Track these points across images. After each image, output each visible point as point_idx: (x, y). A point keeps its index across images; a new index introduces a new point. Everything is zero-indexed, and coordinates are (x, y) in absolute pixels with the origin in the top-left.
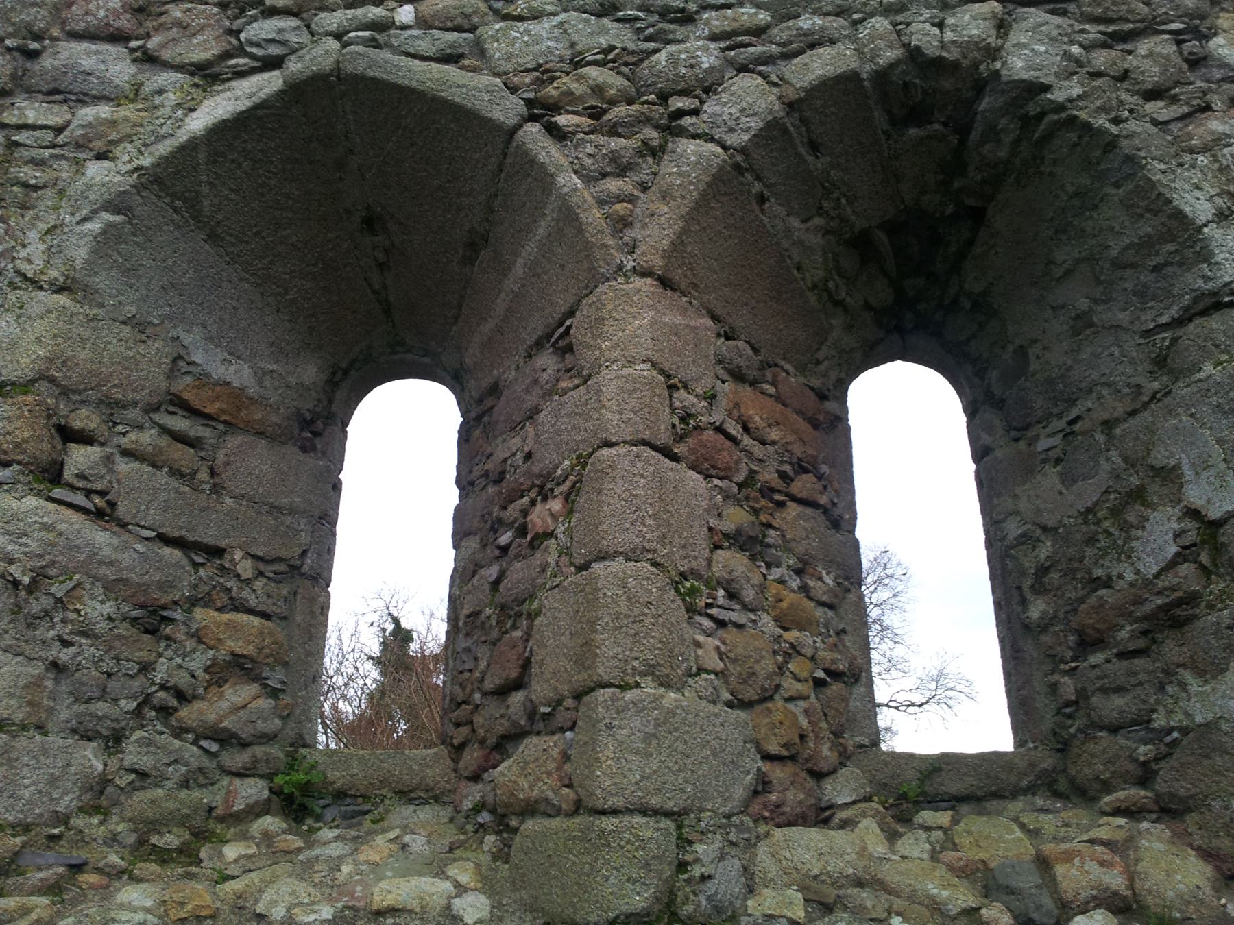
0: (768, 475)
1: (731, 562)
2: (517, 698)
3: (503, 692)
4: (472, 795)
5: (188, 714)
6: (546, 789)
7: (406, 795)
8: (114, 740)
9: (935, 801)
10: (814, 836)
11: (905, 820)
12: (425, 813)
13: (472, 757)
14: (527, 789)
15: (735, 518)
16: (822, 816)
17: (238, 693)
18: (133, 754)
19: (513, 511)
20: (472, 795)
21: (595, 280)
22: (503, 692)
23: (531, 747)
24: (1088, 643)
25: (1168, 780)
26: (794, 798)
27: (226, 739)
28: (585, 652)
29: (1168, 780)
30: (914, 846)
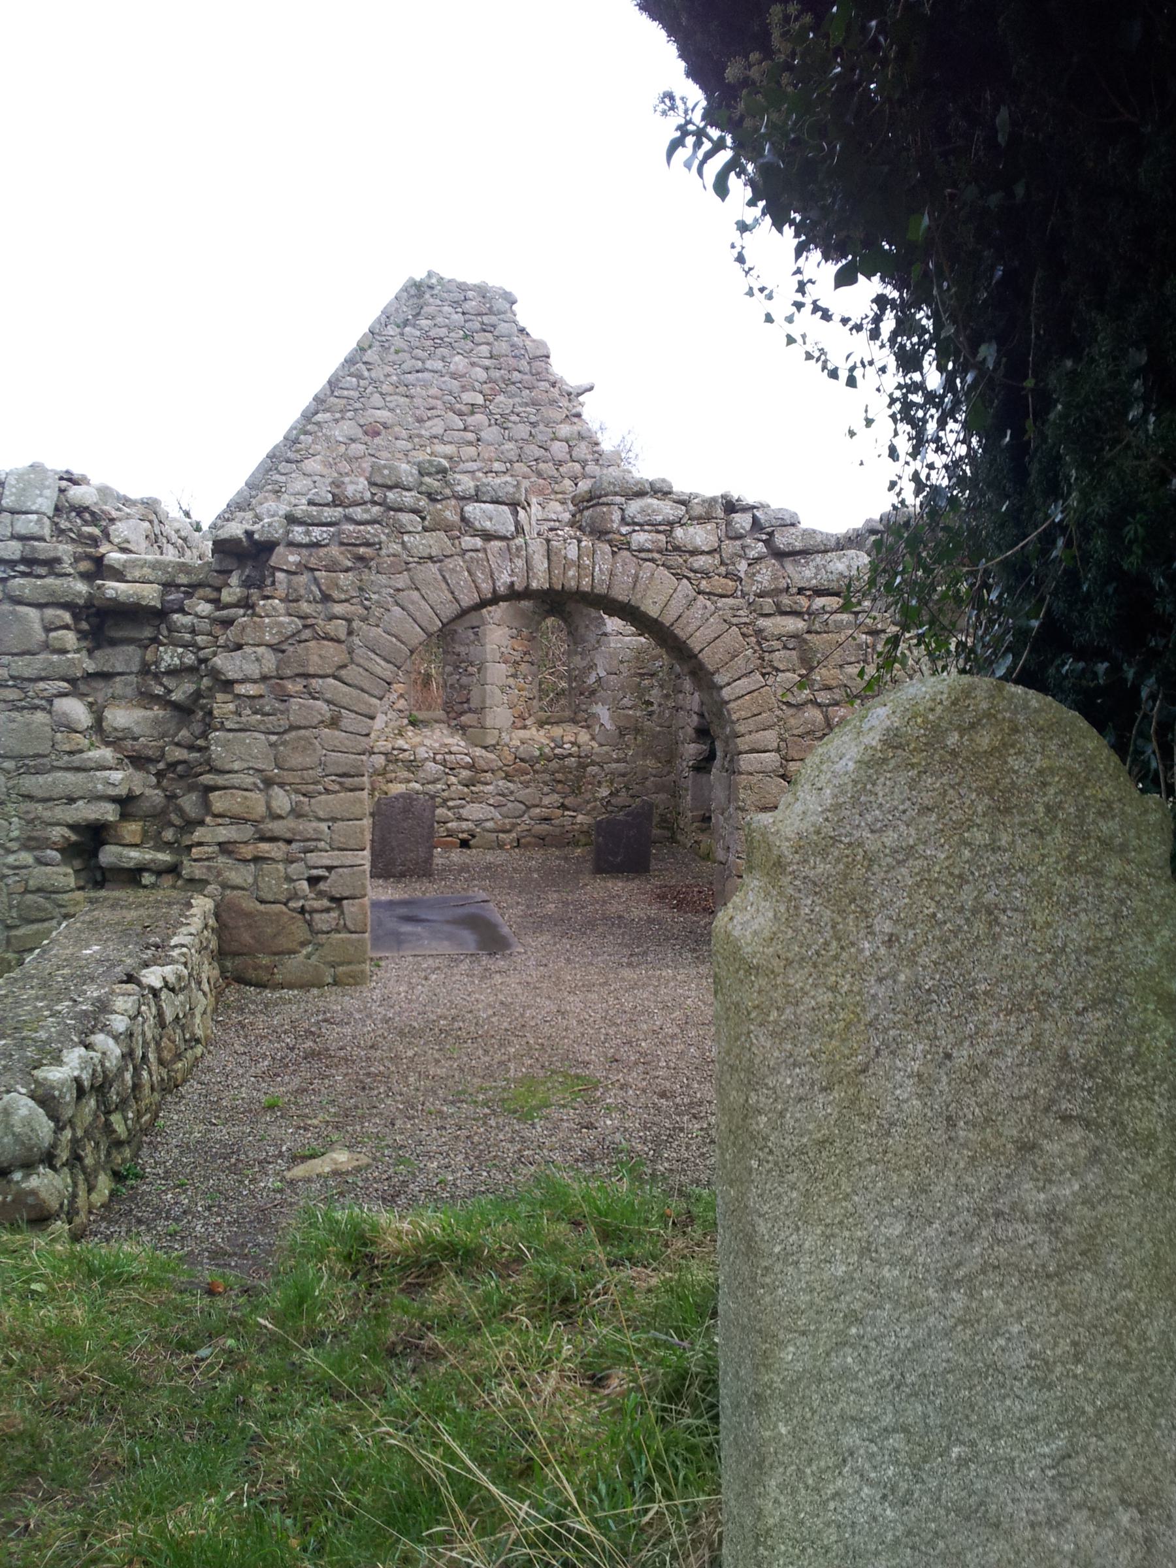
0: (518, 659)
1: (511, 681)
2: (466, 705)
3: (462, 703)
4: (453, 723)
5: (395, 707)
6: (475, 724)
7: (436, 721)
8: (386, 714)
9: (548, 724)
10: (522, 731)
11: (542, 727)
12: (442, 725)
13: (452, 715)
14: (469, 723)
15: (512, 670)
16: (525, 727)
17: (402, 701)
18: (389, 716)
19: (463, 665)
20: (453, 723)
21: (484, 624)
22: (462, 703)
23: (469, 715)
24: (582, 694)
25: (589, 722)
26: (519, 725)
27: (400, 711)
28: (484, 701)
29: (589, 722)
30: (542, 732)
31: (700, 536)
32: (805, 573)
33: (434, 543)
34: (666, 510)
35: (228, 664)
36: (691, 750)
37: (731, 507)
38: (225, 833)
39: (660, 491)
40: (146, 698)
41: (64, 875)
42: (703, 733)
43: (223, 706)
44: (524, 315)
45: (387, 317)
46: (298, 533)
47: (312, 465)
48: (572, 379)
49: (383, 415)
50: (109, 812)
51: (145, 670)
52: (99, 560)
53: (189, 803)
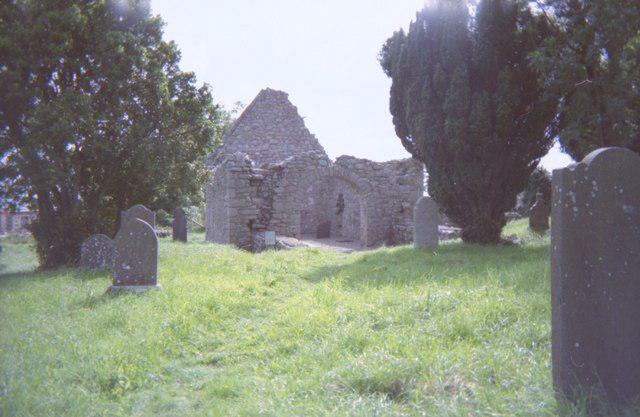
31: (360, 166)
32: (378, 173)
33: (313, 167)
34: (354, 161)
35: (276, 190)
36: (336, 209)
37: (366, 161)
38: (275, 221)
39: (353, 158)
40: (258, 196)
41: (248, 229)
42: (338, 205)
43: (275, 198)
44: (291, 99)
45: (256, 100)
46: (289, 166)
47: (239, 137)
48: (302, 116)
49: (257, 124)
50: (255, 217)
51: (259, 191)
52: (250, 171)
53: (268, 216)
